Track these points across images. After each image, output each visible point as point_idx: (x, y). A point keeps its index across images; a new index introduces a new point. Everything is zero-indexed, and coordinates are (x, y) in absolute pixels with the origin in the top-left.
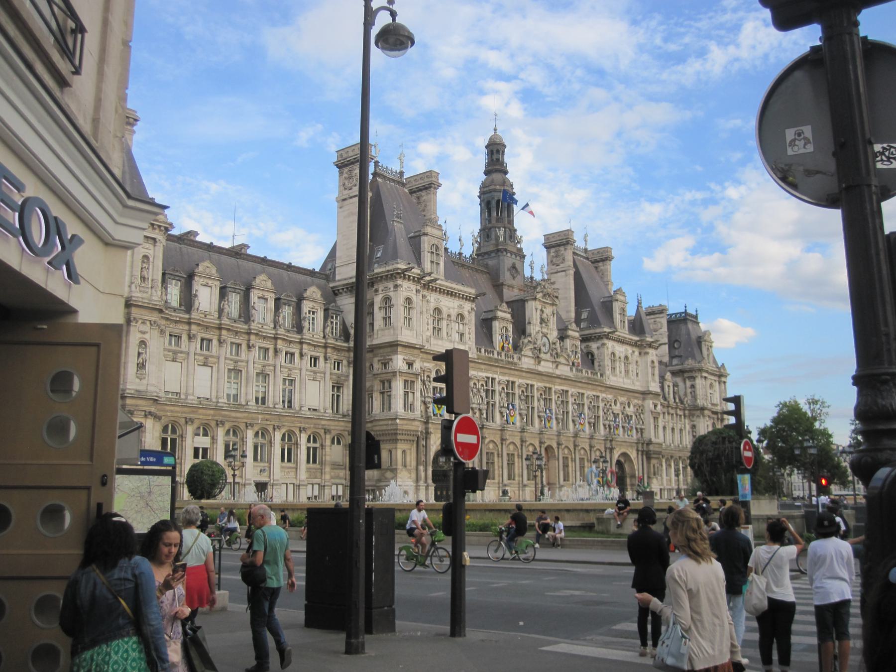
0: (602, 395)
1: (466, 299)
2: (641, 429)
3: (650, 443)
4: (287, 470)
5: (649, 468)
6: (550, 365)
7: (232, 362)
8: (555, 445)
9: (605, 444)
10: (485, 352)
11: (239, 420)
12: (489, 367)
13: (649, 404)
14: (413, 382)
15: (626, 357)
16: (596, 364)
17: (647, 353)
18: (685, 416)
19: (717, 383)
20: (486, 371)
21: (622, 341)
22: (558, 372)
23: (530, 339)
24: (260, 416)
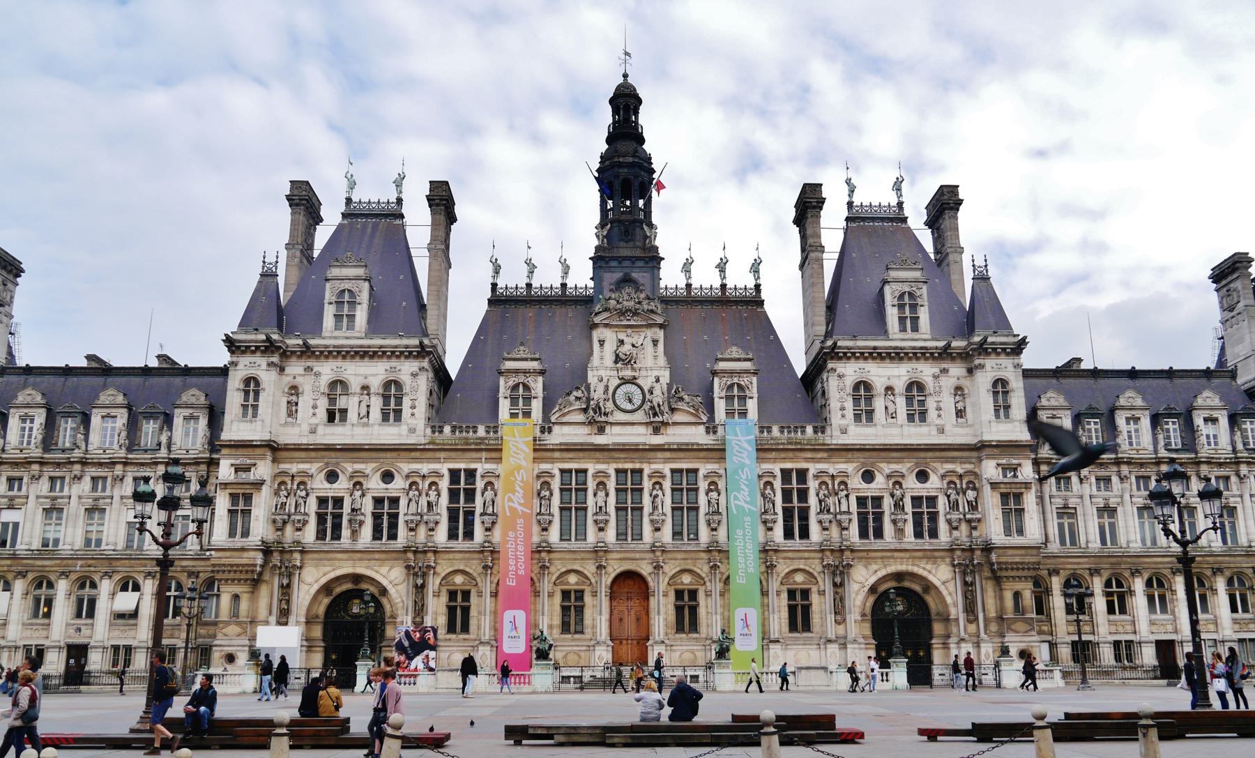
0: (813, 468)
1: (407, 357)
2: (969, 521)
3: (988, 548)
4: (122, 628)
5: (1001, 598)
6: (642, 430)
7: (48, 500)
8: (645, 569)
9: (822, 559)
10: (453, 432)
11: (48, 569)
12: (460, 453)
13: (990, 469)
14: (252, 494)
15: (915, 388)
16: (828, 408)
17: (982, 367)
20: (446, 460)
21: (897, 356)
23: (579, 394)
24: (80, 563)
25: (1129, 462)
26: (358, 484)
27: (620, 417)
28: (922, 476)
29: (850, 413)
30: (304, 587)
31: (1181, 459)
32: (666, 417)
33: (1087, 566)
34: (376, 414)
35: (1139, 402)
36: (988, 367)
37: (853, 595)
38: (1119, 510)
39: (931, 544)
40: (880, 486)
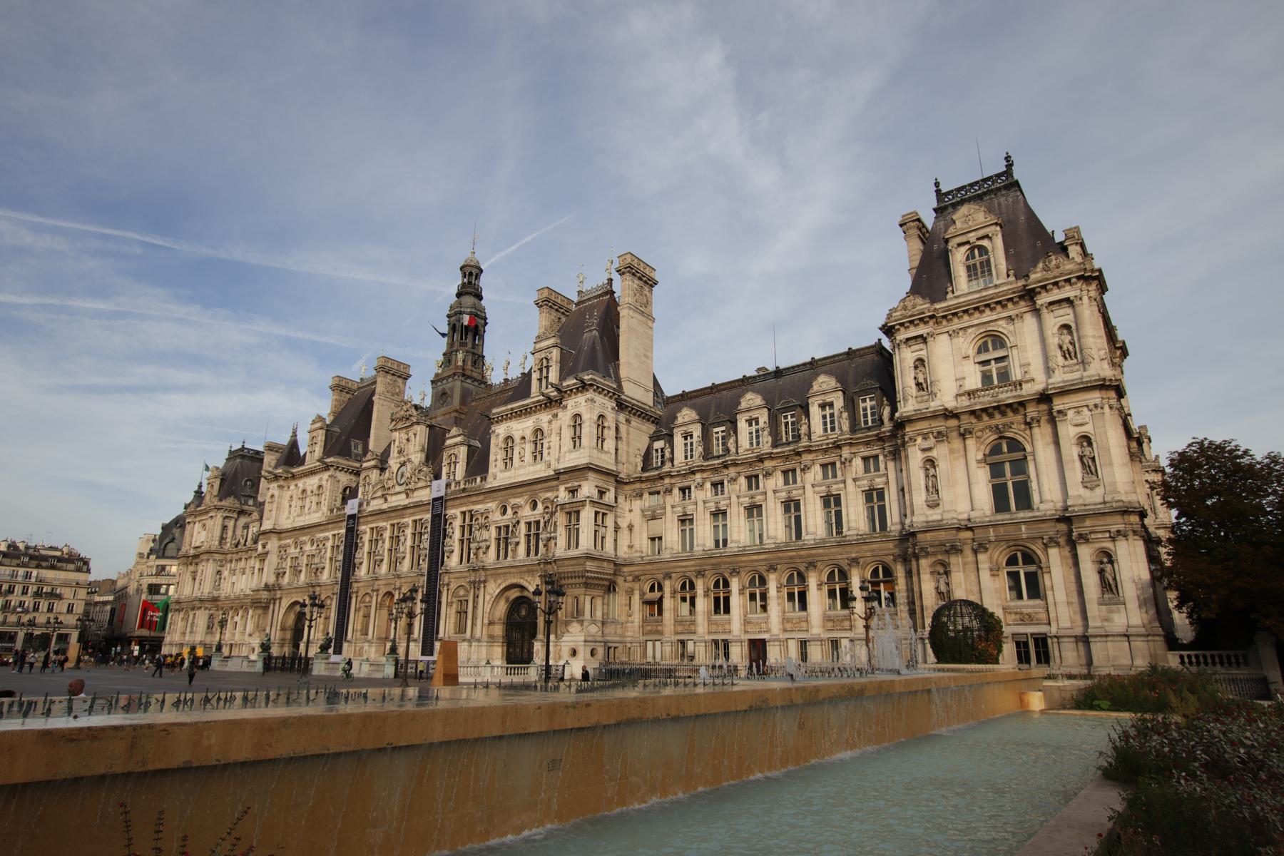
0: (476, 507)
6: (403, 496)
13: (563, 495)
15: (538, 431)
18: (885, 456)
19: (1030, 321)
20: (333, 529)
22: (406, 502)
25: (735, 464)
26: (301, 548)
27: (398, 489)
28: (534, 506)
29: (500, 464)
30: (281, 609)
31: (783, 452)
32: (412, 486)
33: (693, 569)
34: (314, 505)
35: (757, 400)
36: (569, 407)
37: (486, 604)
38: (728, 511)
39: (532, 560)
40: (508, 517)
